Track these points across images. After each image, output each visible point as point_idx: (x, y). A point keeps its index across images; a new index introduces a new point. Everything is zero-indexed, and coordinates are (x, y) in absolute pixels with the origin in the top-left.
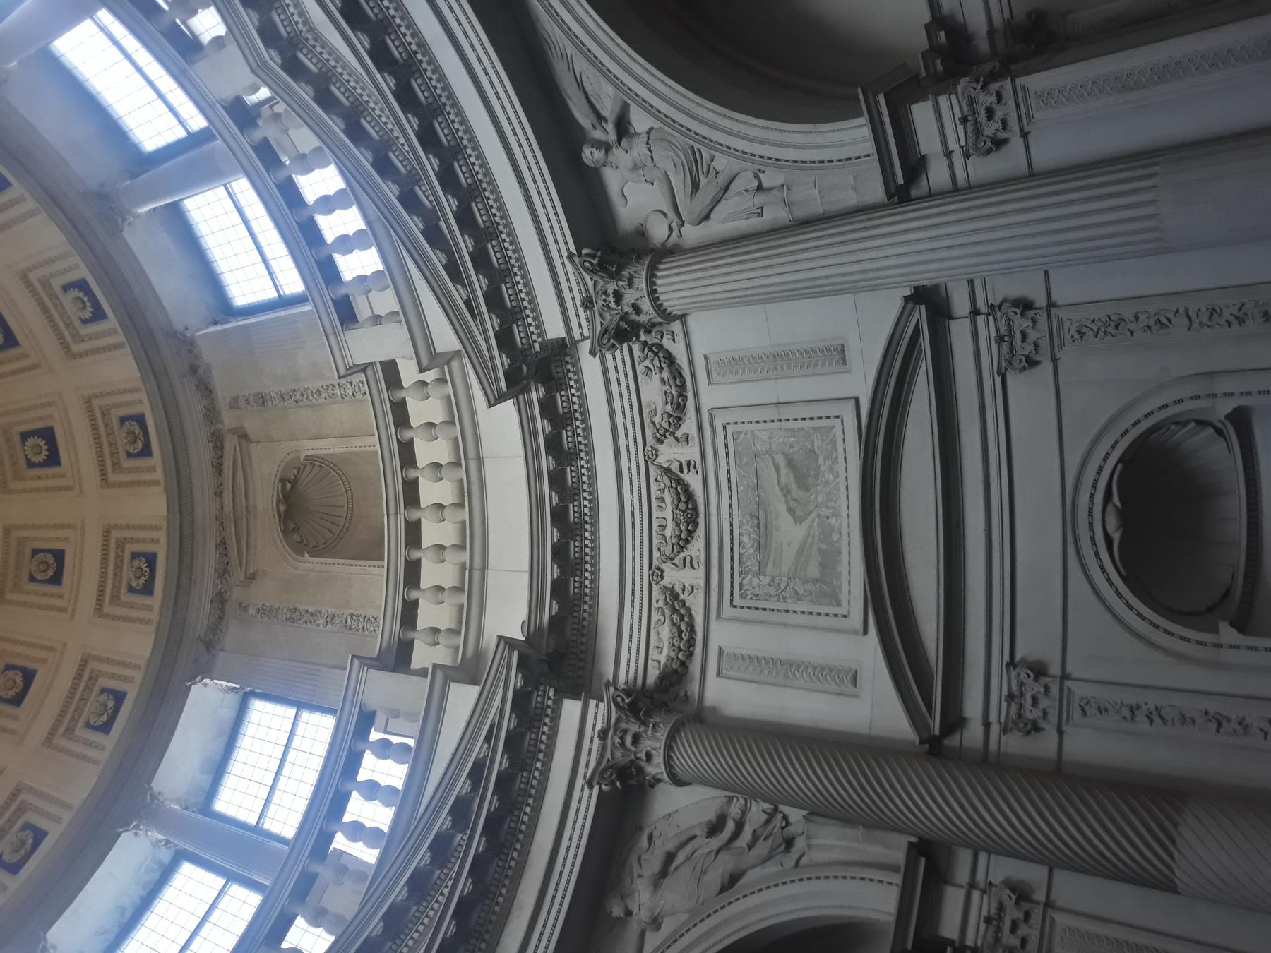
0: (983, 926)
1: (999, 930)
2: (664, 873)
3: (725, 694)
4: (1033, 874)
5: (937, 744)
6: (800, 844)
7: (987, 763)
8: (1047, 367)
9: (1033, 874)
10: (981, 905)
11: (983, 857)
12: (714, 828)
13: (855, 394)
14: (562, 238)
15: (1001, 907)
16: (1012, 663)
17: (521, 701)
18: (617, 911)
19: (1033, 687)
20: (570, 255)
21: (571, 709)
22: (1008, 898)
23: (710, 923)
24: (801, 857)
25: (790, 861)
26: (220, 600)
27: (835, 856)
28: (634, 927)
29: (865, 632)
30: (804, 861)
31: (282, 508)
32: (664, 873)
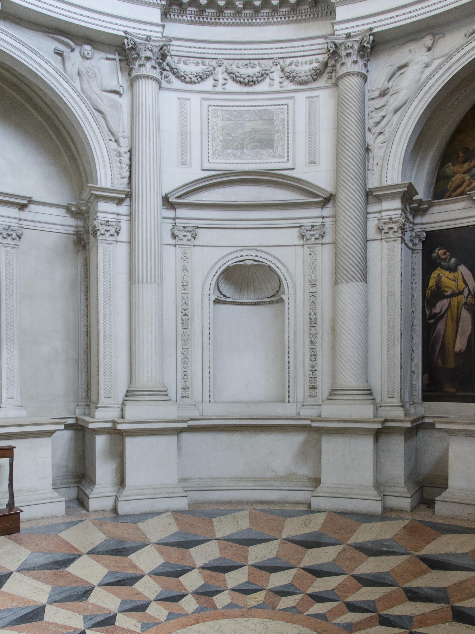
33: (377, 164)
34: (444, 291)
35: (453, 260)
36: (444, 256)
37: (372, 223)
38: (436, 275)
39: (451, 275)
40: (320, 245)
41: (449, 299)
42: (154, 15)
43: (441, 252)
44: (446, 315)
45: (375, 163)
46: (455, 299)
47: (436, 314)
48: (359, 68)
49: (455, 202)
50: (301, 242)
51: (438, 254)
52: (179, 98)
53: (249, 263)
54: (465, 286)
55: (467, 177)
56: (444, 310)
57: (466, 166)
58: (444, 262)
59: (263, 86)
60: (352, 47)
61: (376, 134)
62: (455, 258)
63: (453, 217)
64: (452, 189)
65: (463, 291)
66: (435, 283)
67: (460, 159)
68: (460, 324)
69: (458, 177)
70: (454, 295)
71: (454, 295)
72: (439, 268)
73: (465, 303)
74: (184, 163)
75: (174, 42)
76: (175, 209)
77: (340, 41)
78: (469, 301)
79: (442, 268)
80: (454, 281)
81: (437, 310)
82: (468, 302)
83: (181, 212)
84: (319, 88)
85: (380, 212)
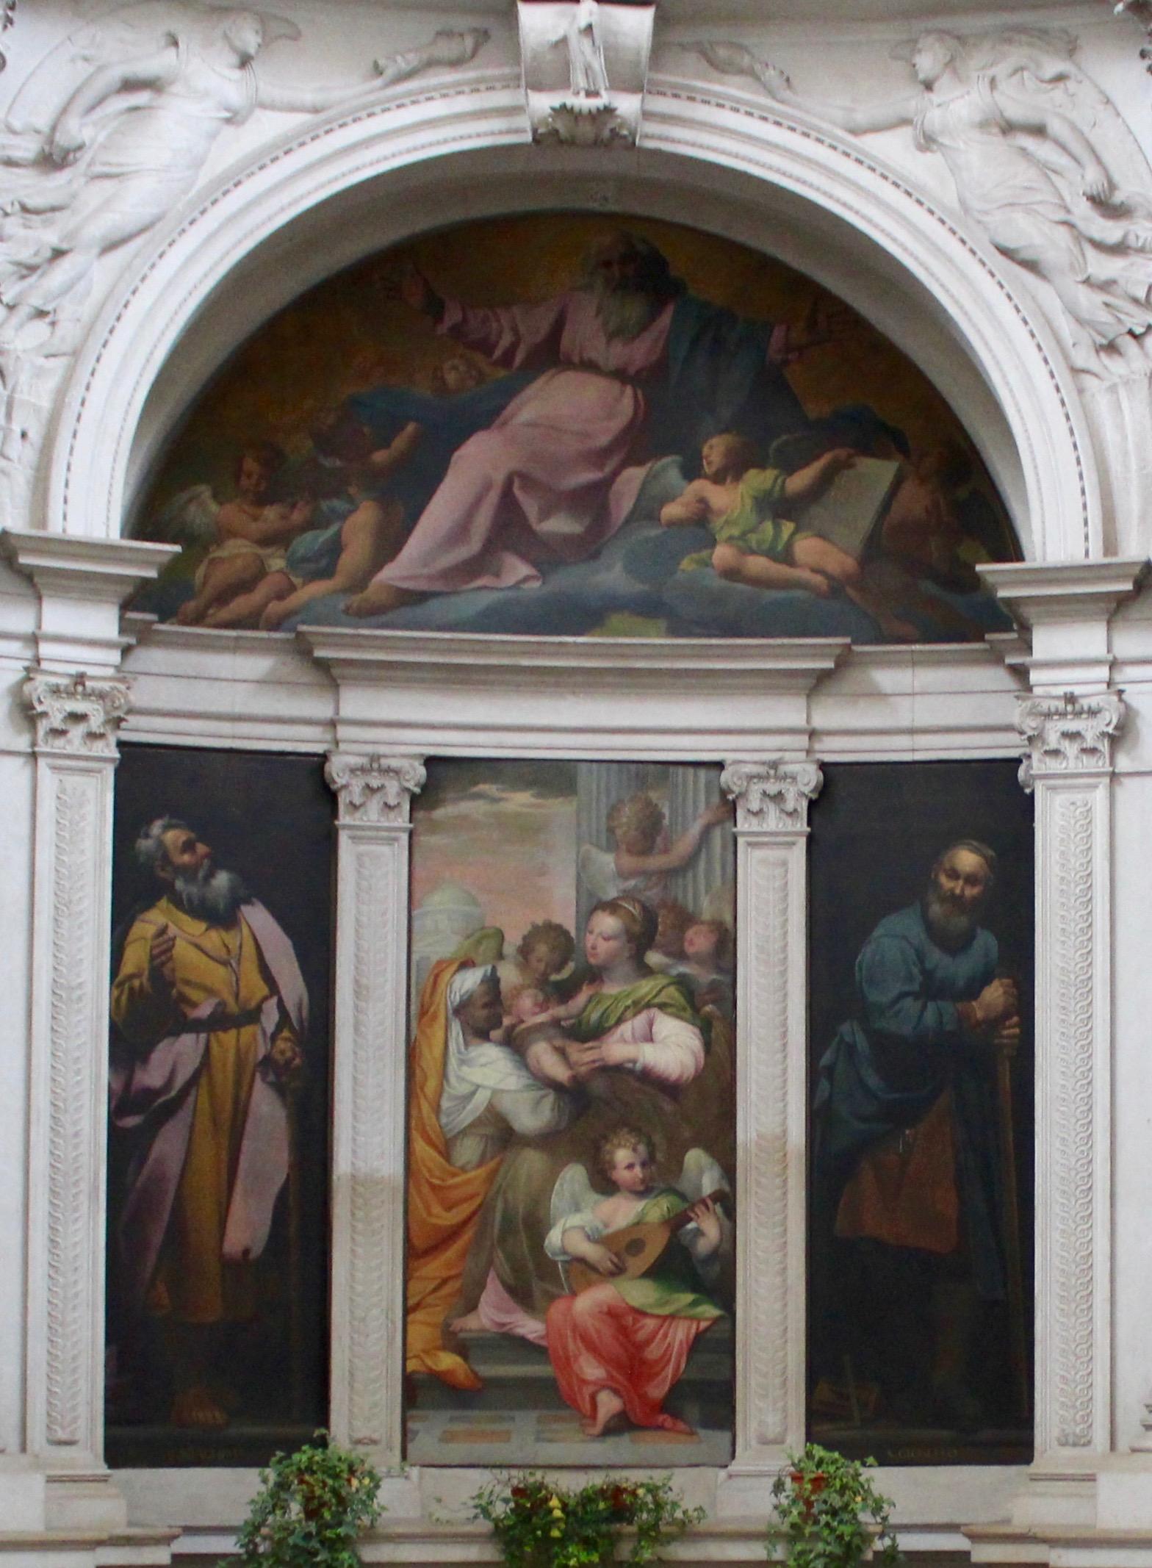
0: (1060, 691)
1: (1063, 715)
2: (1009, 128)
6: (1115, 366)
10: (1088, 685)
12: (1105, 205)
15: (1093, 713)
18: (927, 62)
22: (1109, 718)
23: (953, 246)
24: (1096, 375)
25: (1083, 357)
27: (1110, 436)
28: (908, 100)
30: (1089, 381)
32: (1009, 128)
33: (24, 435)
34: (183, 999)
35: (222, 880)
36: (186, 858)
38: (151, 930)
39: (214, 939)
41: (203, 1036)
43: (174, 837)
44: (191, 1099)
45: (17, 429)
46: (229, 1038)
47: (150, 1093)
49: (236, 647)
51: (160, 843)
54: (265, 991)
55: (277, 563)
56: (180, 1081)
57: (271, 514)
58: (187, 881)
61: (24, 311)
62: (229, 868)
63: (223, 707)
64: (208, 592)
65: (259, 1009)
66: (146, 966)
67: (245, 482)
68: (246, 1145)
69: (237, 552)
70: (220, 1021)
71: (220, 1021)
72: (163, 903)
73: (268, 1059)
78: (282, 1052)
79: (178, 902)
80: (225, 963)
81: (152, 1076)
82: (278, 1056)
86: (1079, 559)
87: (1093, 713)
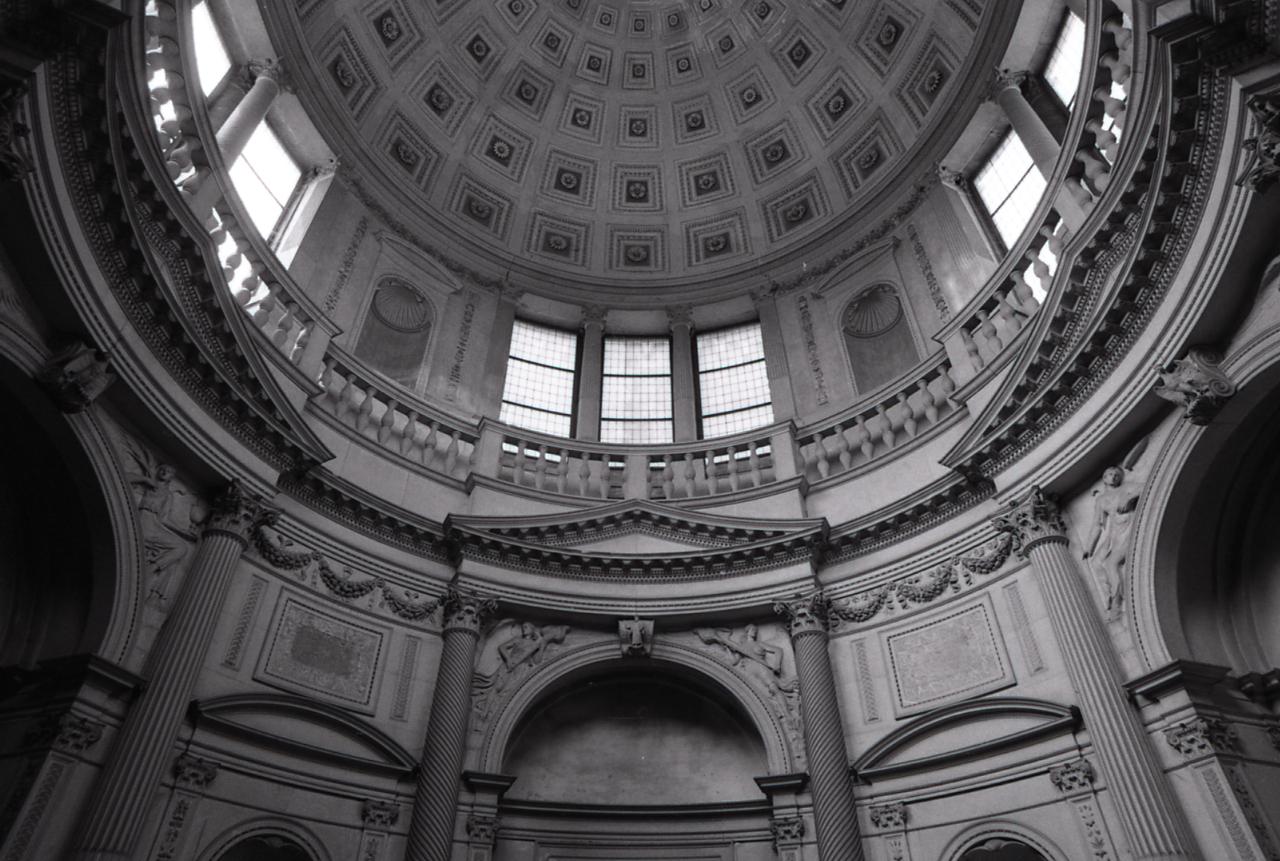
1: (784, 825)
3: (845, 648)
4: (811, 836)
5: (856, 776)
7: (853, 804)
8: (1061, 795)
9: (811, 836)
11: (811, 809)
13: (1019, 682)
14: (1046, 478)
16: (905, 804)
17: (799, 542)
19: (897, 817)
20: (1037, 487)
21: (805, 569)
26: (800, 282)
29: (898, 719)
31: (865, 294)
37: (462, 818)
40: (386, 835)
42: (272, 475)
48: (474, 627)
50: (359, 823)
52: (255, 576)
53: (278, 843)
59: (361, 602)
60: (474, 605)
74: (229, 664)
75: (282, 516)
76: (194, 728)
77: (463, 594)
83: (201, 736)
84: (424, 630)
85: (472, 805)
86: (783, 773)
87: (794, 824)
